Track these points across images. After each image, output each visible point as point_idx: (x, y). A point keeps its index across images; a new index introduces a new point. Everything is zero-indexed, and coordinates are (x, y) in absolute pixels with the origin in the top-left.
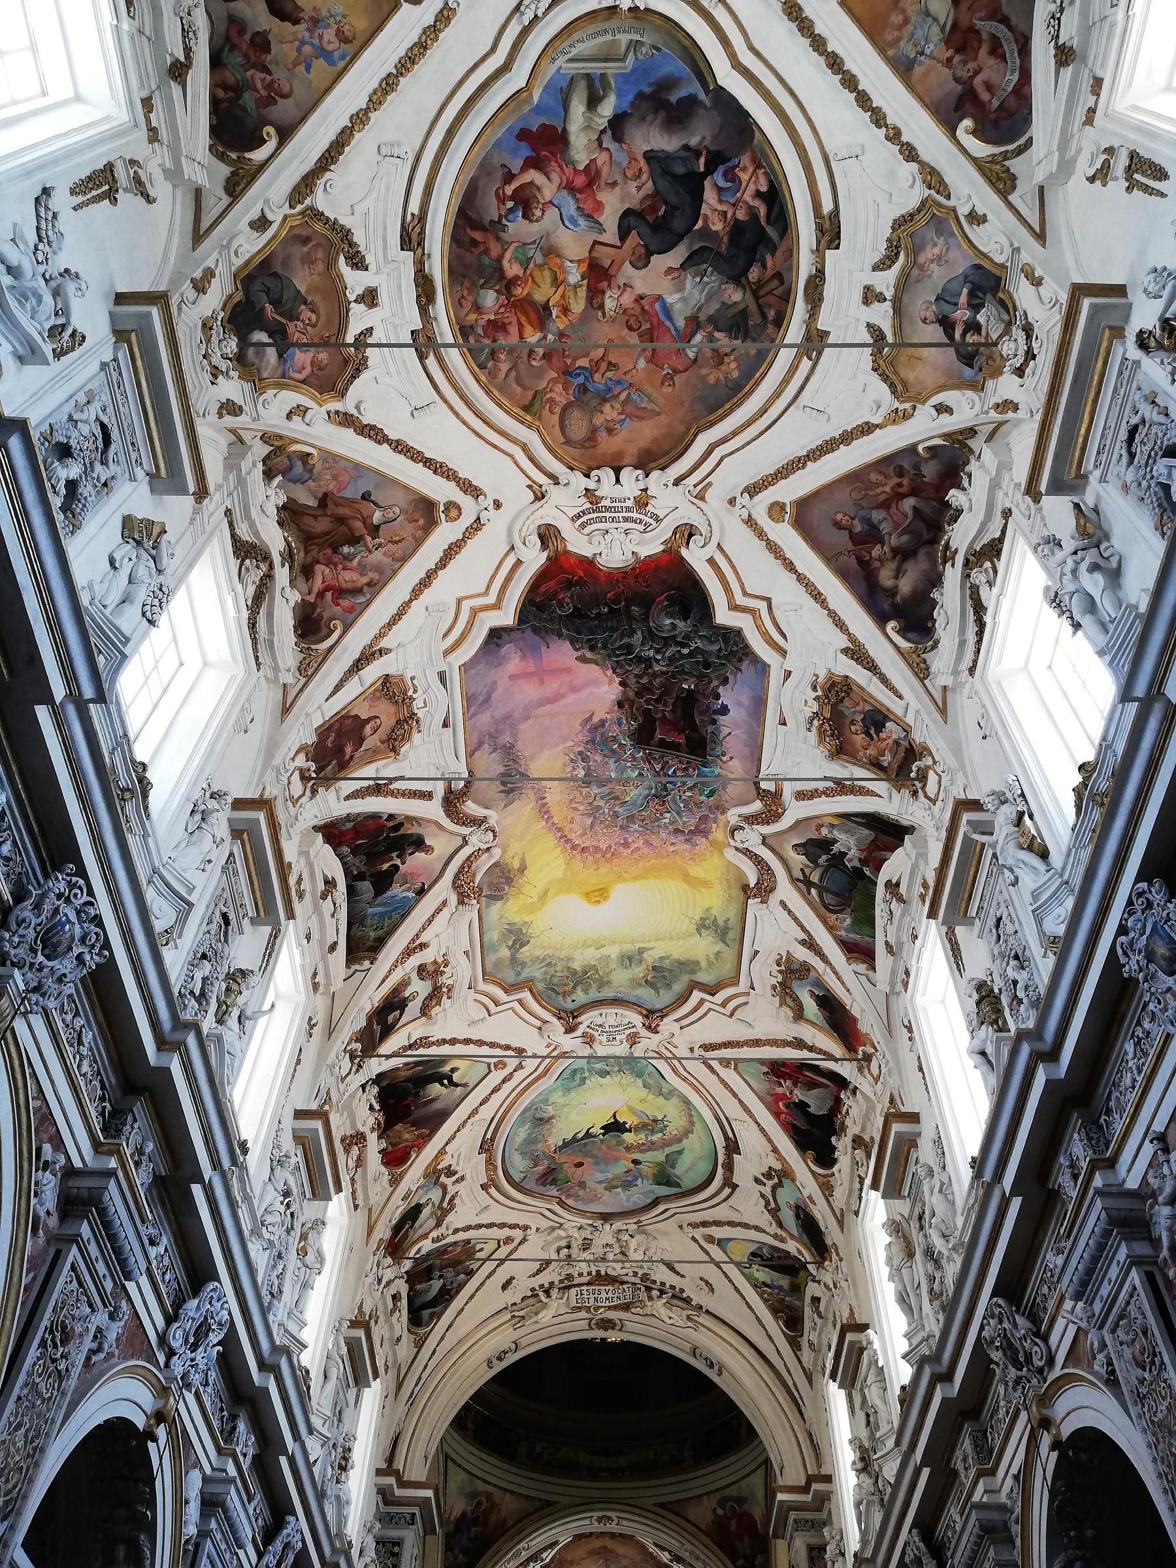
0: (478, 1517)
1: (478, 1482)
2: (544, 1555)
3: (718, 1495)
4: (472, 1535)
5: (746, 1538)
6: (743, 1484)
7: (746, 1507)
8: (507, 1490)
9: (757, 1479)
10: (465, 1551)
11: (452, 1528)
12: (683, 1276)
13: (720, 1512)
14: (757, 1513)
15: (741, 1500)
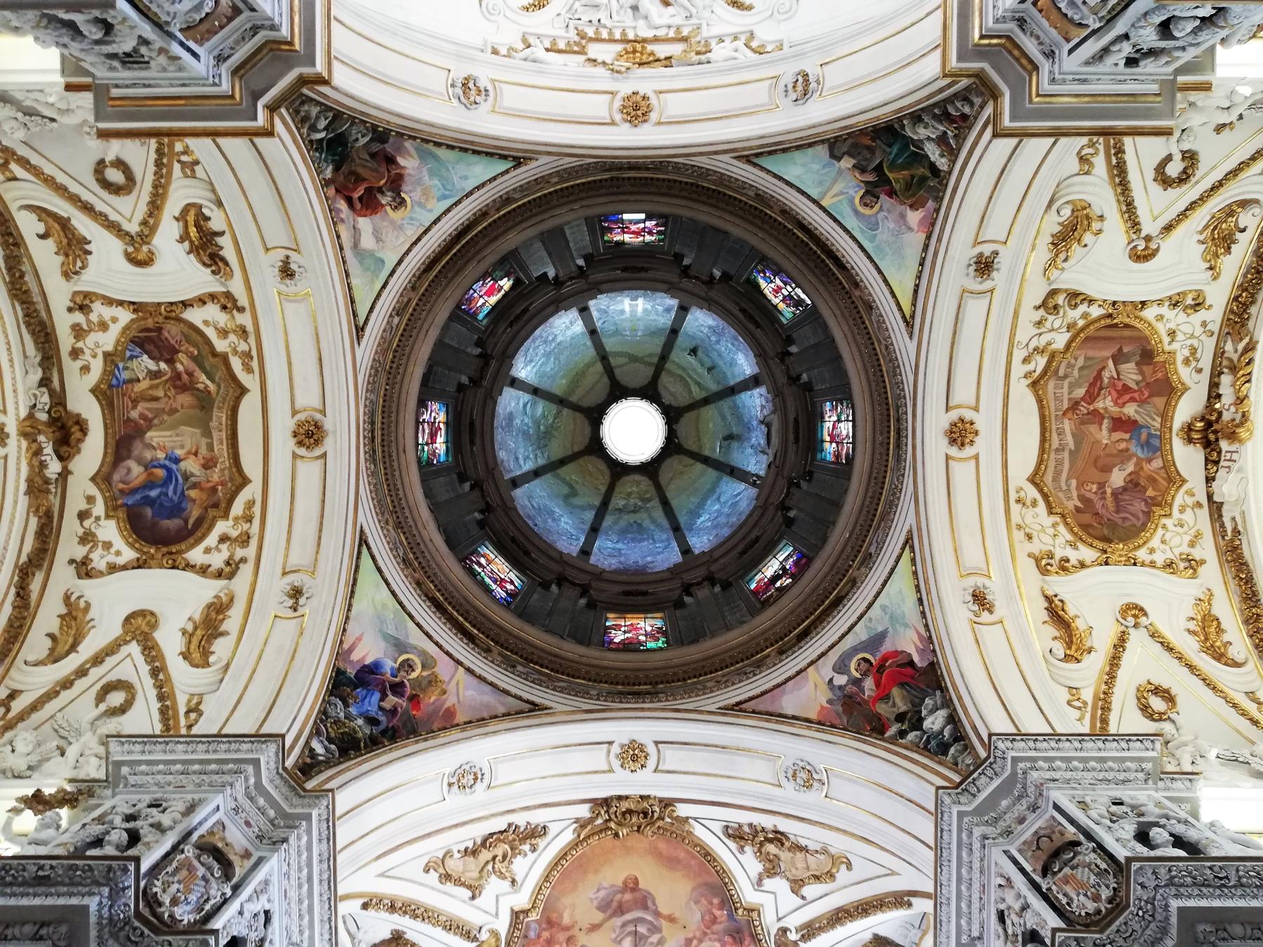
0: (402, 684)
1: (411, 624)
2: (520, 865)
3: (833, 656)
4: (387, 705)
5: (896, 692)
6: (875, 611)
7: (887, 647)
8: (459, 663)
9: (901, 585)
10: (372, 721)
11: (351, 672)
12: (750, 8)
13: (841, 680)
14: (907, 642)
15: (877, 640)
